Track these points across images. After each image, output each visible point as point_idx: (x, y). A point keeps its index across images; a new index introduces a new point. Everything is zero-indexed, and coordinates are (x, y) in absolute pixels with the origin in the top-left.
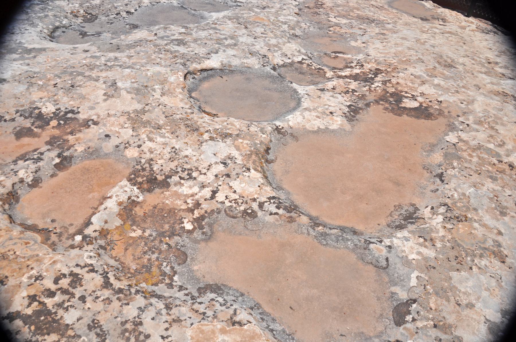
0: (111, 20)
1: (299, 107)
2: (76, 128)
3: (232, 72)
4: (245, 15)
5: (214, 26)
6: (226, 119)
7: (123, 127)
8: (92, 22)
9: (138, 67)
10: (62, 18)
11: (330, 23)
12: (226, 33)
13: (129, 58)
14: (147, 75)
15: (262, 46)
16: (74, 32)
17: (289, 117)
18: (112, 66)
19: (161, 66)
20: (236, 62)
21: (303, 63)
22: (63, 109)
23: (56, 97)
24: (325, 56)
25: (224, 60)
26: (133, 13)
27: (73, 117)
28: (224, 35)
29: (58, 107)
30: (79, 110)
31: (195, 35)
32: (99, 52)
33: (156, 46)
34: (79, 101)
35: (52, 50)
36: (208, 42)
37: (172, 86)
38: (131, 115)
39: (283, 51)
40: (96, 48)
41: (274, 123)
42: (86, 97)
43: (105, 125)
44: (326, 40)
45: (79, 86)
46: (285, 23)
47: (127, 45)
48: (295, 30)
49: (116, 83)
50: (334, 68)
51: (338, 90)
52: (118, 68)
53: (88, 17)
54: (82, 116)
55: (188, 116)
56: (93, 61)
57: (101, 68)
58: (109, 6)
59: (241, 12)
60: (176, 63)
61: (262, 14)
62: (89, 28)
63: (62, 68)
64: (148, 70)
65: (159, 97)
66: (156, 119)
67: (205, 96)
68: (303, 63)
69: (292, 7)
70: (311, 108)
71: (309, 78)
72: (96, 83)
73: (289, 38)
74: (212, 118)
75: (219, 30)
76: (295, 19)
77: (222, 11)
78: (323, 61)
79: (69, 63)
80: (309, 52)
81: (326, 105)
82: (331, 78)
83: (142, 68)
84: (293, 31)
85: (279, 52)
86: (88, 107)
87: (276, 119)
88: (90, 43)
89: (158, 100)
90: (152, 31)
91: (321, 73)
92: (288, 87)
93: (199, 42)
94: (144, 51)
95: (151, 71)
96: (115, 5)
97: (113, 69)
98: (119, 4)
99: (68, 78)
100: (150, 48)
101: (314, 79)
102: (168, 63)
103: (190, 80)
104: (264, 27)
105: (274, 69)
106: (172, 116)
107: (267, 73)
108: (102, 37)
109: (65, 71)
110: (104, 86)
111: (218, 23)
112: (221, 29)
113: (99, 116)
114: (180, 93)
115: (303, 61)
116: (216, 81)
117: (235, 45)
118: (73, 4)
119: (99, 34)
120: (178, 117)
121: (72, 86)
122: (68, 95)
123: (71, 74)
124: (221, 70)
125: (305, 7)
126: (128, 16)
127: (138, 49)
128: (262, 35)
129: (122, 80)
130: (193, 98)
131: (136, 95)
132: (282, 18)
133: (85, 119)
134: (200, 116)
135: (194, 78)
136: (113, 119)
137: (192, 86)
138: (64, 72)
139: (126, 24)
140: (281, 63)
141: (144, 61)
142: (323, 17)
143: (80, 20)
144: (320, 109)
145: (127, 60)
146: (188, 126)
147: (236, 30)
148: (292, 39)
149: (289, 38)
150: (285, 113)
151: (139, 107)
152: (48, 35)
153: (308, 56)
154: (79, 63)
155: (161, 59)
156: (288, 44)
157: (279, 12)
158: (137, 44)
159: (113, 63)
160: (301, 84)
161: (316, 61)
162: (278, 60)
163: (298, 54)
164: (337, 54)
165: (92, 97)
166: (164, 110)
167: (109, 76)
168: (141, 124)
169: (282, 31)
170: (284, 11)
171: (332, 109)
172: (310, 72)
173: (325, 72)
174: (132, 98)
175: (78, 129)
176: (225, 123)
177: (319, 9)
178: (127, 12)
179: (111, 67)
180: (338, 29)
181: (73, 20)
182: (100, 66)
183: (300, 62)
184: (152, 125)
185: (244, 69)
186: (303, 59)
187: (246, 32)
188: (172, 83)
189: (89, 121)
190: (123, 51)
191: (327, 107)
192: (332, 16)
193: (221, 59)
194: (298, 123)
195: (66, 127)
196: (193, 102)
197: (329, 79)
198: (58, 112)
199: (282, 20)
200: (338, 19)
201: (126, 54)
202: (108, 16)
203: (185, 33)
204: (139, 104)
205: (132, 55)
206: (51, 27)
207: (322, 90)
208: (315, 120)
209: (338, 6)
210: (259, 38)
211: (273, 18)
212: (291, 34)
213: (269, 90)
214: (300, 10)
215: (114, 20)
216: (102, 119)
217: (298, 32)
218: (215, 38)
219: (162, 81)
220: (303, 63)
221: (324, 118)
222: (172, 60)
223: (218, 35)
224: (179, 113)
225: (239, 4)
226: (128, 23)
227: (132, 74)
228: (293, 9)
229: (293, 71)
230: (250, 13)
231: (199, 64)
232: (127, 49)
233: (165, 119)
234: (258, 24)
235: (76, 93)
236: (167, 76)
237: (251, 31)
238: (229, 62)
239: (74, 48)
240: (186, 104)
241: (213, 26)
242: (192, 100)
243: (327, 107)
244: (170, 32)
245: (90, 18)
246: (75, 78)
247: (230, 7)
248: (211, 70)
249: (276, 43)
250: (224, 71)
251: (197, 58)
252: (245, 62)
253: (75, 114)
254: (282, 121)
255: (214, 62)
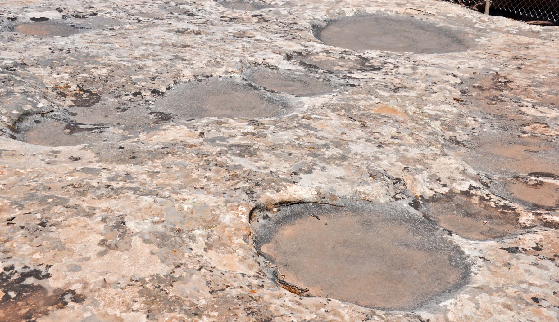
0: (124, 104)
1: (467, 283)
2: (38, 308)
3: (336, 208)
4: (362, 103)
5: (305, 123)
6: (323, 300)
7: (129, 309)
8: (90, 106)
9: (167, 193)
10: (38, 97)
11: (524, 117)
12: (326, 136)
13: (151, 176)
14: (181, 209)
15: (394, 160)
16: (56, 123)
17: (447, 302)
18: (119, 189)
19: (209, 193)
20: (344, 191)
21: (471, 196)
22: (19, 268)
23: (8, 245)
24: (515, 181)
25: (323, 185)
26: (163, 93)
27: (36, 284)
28: (323, 138)
29: (9, 263)
30: (50, 271)
31: (271, 138)
32: (98, 161)
33: (200, 155)
34: (52, 253)
35: (13, 154)
36: (293, 151)
37: (226, 232)
38: (148, 286)
39: (433, 171)
40: (93, 155)
41: (417, 313)
42: (66, 246)
43: (95, 303)
44: (518, 150)
45: (54, 225)
46: (436, 118)
47: (149, 152)
48: (455, 131)
49: (124, 223)
50: (536, 206)
51: (547, 251)
52: (130, 193)
53: (84, 96)
54: (52, 285)
55: (253, 292)
56: (86, 178)
57: (100, 192)
58: (123, 80)
59: (355, 97)
60: (235, 189)
61: (392, 101)
62: (84, 117)
63: (28, 188)
64: (185, 200)
65: (201, 252)
66: (192, 296)
67: (285, 253)
68: (471, 196)
69: (449, 87)
70: (493, 287)
71: (484, 224)
72: (89, 221)
73: (443, 146)
74: (297, 298)
75: (315, 129)
76: (455, 110)
77: (320, 94)
78: (512, 191)
79: (41, 180)
80: (482, 173)
81: (522, 282)
82: (531, 227)
83: (174, 196)
84: (451, 133)
85: (426, 174)
86: (68, 266)
87: (421, 306)
88: (83, 145)
89: (198, 258)
90: (196, 128)
91: (507, 215)
92: (443, 241)
93: (278, 151)
94: (180, 163)
95: (190, 201)
96: (134, 77)
97: (120, 195)
98: (141, 77)
99: (37, 208)
100: (191, 160)
101: (495, 227)
102: (221, 188)
103: (260, 220)
104: (397, 125)
105: (416, 205)
106: (223, 290)
107: (402, 212)
108: (105, 134)
109: (32, 195)
110: (102, 227)
111: (313, 116)
112: (319, 128)
113: (86, 285)
114: (241, 246)
115: (472, 192)
116: (307, 226)
117: (344, 158)
118: (58, 73)
119: (100, 128)
120: (234, 292)
121: (43, 224)
122: (32, 241)
123: (43, 200)
124: (316, 203)
125: (474, 87)
126: (153, 99)
127: (169, 159)
128: (393, 140)
129: (136, 217)
130: (263, 256)
131: (159, 246)
132: (429, 109)
133: (59, 290)
134: (276, 293)
135: (266, 217)
136: (111, 291)
137: (262, 232)
138: (31, 197)
139: (149, 111)
140: (429, 194)
141: (179, 182)
142: (510, 105)
143: (69, 101)
144: (510, 291)
145: (148, 179)
146: (252, 313)
147: (346, 130)
148: (449, 147)
149: (443, 146)
150: (439, 294)
151: (162, 269)
152: (9, 127)
153: (480, 181)
154: (60, 181)
155: (208, 179)
156: (442, 159)
157: (424, 98)
158: (168, 150)
159: (121, 184)
160: (470, 236)
161: (497, 192)
162: (423, 188)
163: (460, 177)
164: (541, 179)
165: (77, 248)
166: (209, 278)
167: (113, 209)
168: (165, 304)
169: (430, 133)
170: (434, 95)
171: (536, 292)
172: (486, 212)
173: (518, 215)
174: (152, 253)
175: (43, 309)
176: (323, 310)
177: (501, 90)
178: (154, 91)
179: (117, 191)
180: (540, 128)
181: (57, 102)
182: (98, 188)
183: (466, 194)
184: (184, 307)
185: (359, 204)
186: (471, 187)
187: (363, 133)
188: (226, 227)
189: (65, 294)
190: (141, 163)
191: (525, 286)
192: (526, 104)
193: (317, 185)
194: (466, 316)
195: (20, 303)
196: (263, 264)
197: (526, 227)
198: (7, 273)
199: (429, 112)
200: (540, 109)
201: (146, 168)
202: (119, 96)
203: (253, 134)
204: (164, 265)
205: (157, 169)
206: (15, 112)
207: (514, 250)
208: (501, 312)
209: (540, 84)
210: (387, 145)
211: (413, 109)
212: (447, 137)
213: (407, 245)
214: (464, 92)
215: (130, 104)
216: (91, 291)
217: (461, 134)
218: (307, 144)
219: (209, 222)
220: (473, 195)
221: (519, 308)
222: (228, 183)
223: (313, 139)
224: (236, 285)
225: (351, 82)
226: (153, 110)
227: (155, 205)
228: (451, 92)
229: (452, 209)
230: (371, 99)
231: (278, 191)
232: (149, 159)
233: (209, 295)
234: (386, 119)
235: (48, 239)
236: (217, 212)
237: (372, 133)
238: (332, 189)
239: (54, 152)
240: (250, 267)
241: (304, 121)
242: (261, 259)
243: (525, 286)
244: (227, 131)
245: (87, 98)
246: (49, 210)
247: (335, 87)
248: (298, 203)
249: (419, 157)
250: (322, 206)
251: (274, 181)
252: (362, 190)
253: (40, 279)
254: (434, 311)
255: (304, 190)
